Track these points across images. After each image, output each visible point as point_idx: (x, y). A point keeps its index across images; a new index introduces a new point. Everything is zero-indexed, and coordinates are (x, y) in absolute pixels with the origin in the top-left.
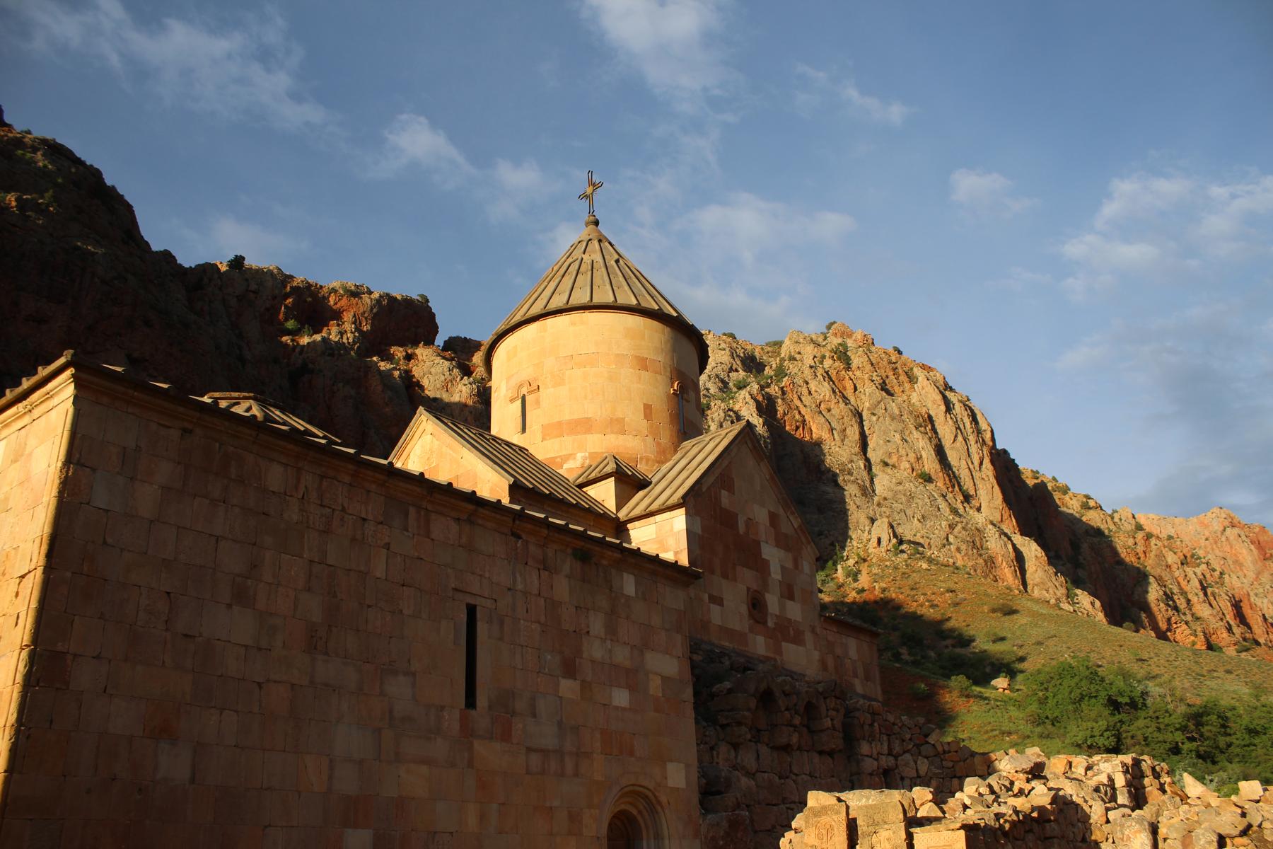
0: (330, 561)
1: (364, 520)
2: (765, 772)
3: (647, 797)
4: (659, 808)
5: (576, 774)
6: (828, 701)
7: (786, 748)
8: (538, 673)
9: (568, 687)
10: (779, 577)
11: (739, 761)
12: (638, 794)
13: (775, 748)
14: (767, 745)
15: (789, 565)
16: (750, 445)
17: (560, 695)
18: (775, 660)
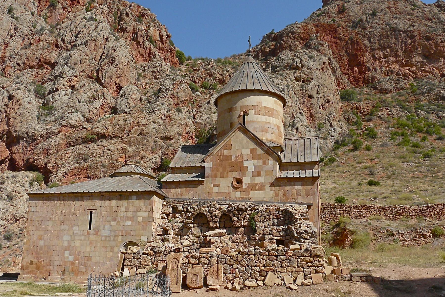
9: (113, 223)
16: (242, 130)
18: (246, 198)
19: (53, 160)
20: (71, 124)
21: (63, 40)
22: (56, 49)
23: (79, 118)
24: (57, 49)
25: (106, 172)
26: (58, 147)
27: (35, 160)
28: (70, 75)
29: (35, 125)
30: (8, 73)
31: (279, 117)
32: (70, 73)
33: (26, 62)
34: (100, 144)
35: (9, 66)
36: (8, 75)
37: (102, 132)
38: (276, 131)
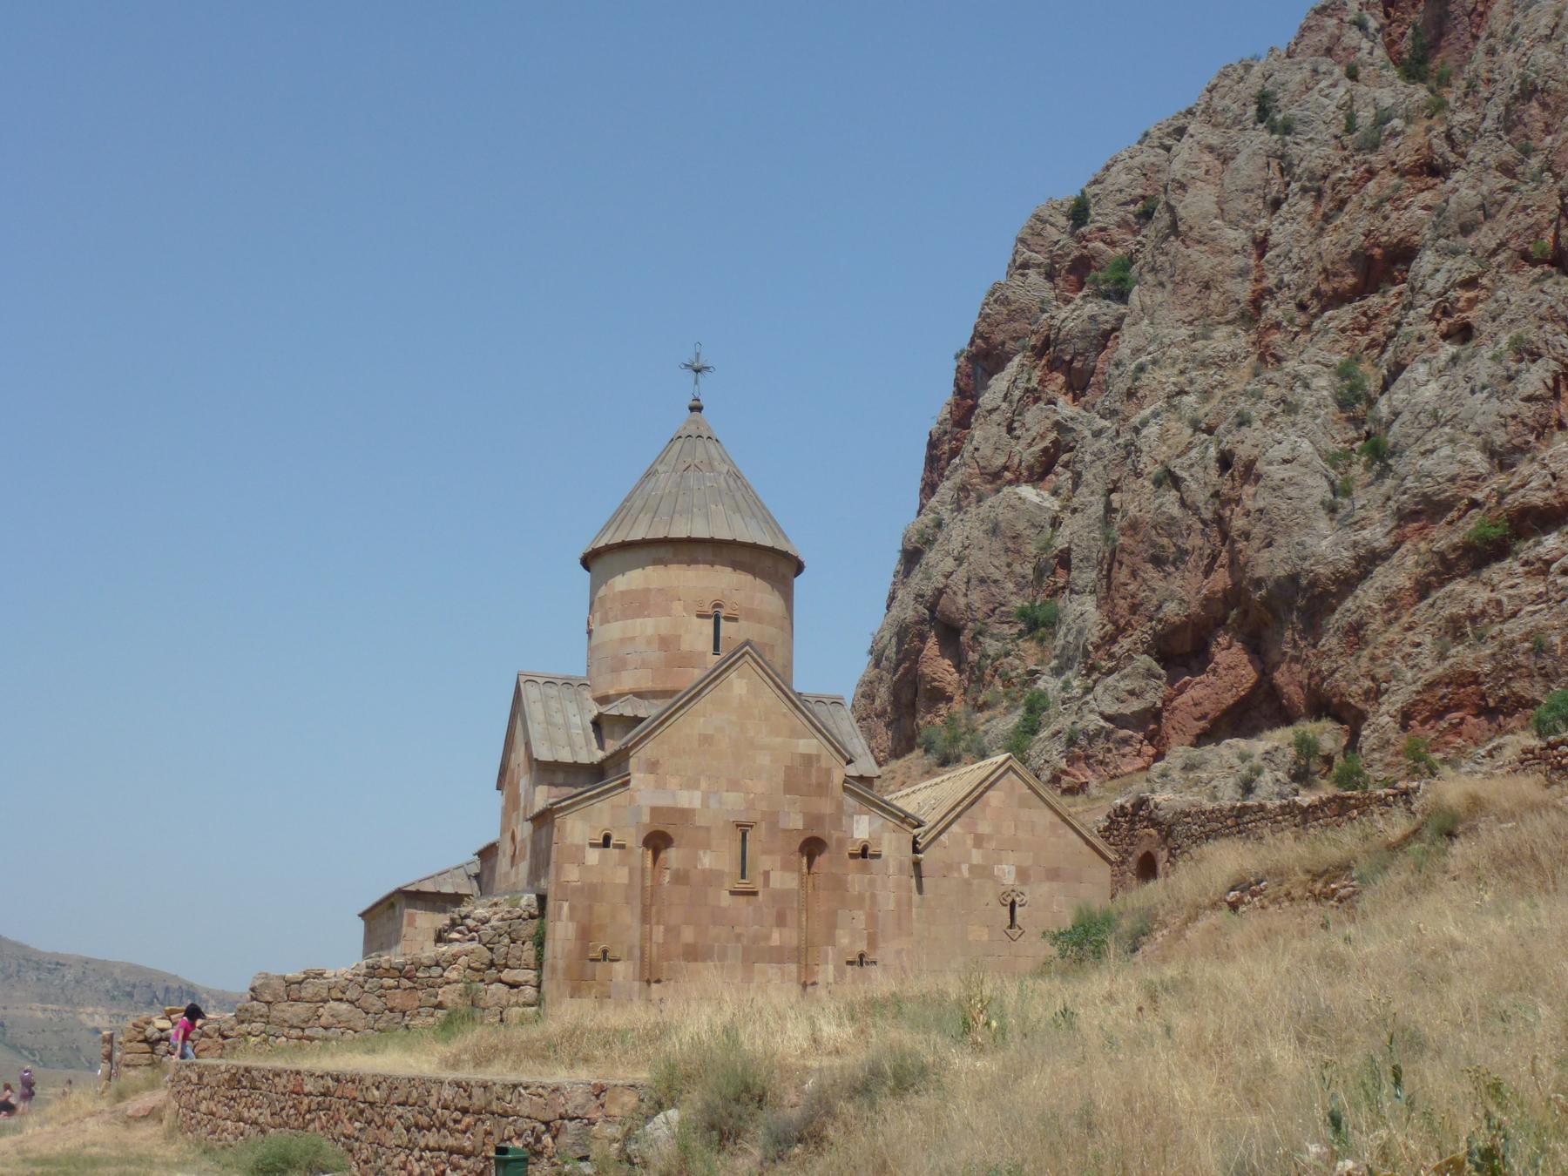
19: (1364, 663)
20: (1436, 498)
21: (1449, 136)
22: (1430, 181)
23: (1463, 463)
24: (1437, 181)
25: (1557, 673)
26: (1390, 609)
27: (1323, 679)
28: (1439, 289)
29: (1315, 541)
30: (1273, 355)
31: (677, 607)
32: (1441, 278)
33: (1325, 287)
34: (1532, 555)
35: (1272, 326)
36: (1272, 361)
37: (1537, 498)
38: (655, 655)
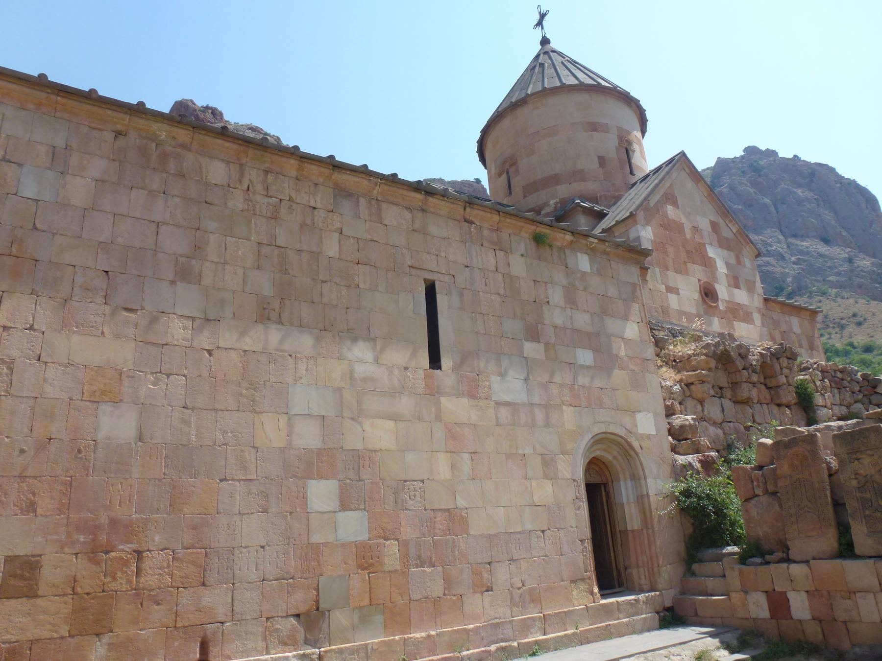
0: (281, 242)
1: (314, 208)
2: (730, 422)
3: (619, 443)
4: (632, 453)
5: (547, 424)
6: (781, 360)
7: (747, 402)
8: (501, 337)
10: (725, 271)
11: (706, 412)
12: (612, 441)
13: (736, 402)
14: (730, 399)
15: (733, 261)
16: (687, 170)
17: (525, 356)
